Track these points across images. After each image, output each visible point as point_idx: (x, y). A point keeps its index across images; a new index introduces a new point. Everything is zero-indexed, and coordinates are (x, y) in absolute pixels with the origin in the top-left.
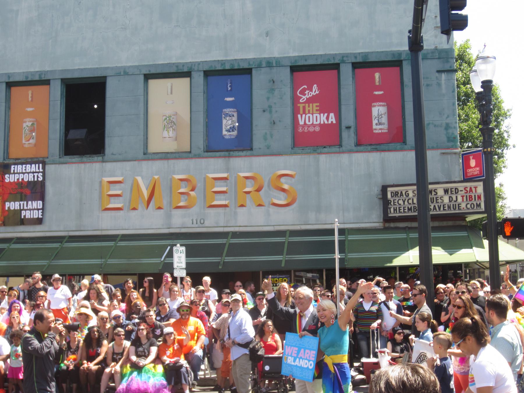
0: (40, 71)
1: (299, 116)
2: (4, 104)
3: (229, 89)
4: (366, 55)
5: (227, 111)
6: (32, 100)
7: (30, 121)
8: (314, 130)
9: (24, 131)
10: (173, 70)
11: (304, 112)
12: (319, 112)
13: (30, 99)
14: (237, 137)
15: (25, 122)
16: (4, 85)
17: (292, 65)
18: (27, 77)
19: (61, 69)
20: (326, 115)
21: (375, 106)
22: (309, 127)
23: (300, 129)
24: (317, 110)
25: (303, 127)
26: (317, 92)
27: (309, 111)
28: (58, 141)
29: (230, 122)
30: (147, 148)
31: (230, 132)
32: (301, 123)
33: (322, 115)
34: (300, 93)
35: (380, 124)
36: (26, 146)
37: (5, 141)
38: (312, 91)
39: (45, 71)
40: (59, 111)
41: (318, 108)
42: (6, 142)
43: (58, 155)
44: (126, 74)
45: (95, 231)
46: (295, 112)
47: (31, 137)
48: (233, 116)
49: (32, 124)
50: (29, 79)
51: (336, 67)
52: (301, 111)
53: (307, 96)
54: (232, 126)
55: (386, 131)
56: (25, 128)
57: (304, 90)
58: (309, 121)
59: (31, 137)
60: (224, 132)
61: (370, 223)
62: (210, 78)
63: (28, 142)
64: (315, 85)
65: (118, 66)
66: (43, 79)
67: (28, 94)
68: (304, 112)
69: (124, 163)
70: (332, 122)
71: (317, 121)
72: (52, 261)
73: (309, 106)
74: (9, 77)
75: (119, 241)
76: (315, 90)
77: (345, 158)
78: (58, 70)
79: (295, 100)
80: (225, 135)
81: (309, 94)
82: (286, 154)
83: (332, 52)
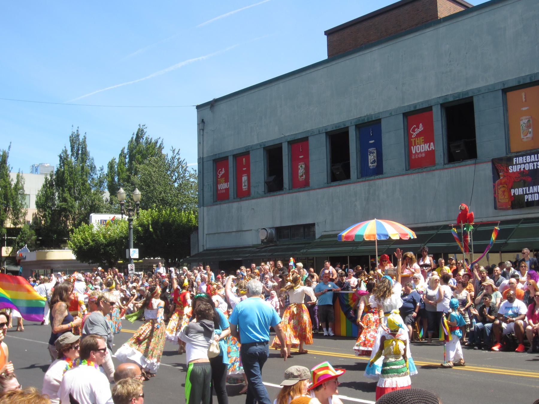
0: (530, 75)
1: (412, 147)
2: (502, 108)
3: (371, 134)
5: (370, 150)
6: (526, 101)
8: (422, 157)
9: (521, 127)
10: (528, 81)
11: (415, 145)
12: (424, 143)
13: (524, 100)
14: (377, 166)
15: (522, 120)
16: (500, 93)
18: (519, 82)
20: (428, 144)
22: (418, 154)
24: (422, 142)
25: (415, 155)
26: (422, 129)
27: (418, 143)
29: (372, 157)
32: (414, 152)
33: (426, 144)
34: (412, 131)
35: (245, 186)
36: (301, 180)
37: (506, 138)
38: (419, 129)
41: (423, 140)
42: (507, 139)
44: (391, 115)
46: (409, 145)
48: (374, 153)
49: (528, 121)
50: (521, 83)
51: (429, 109)
52: (413, 144)
54: (374, 159)
55: (247, 189)
56: (522, 125)
57: (415, 128)
58: (418, 150)
60: (370, 165)
61: (446, 221)
63: (527, 137)
64: (421, 124)
65: (264, 141)
69: (356, 184)
70: (432, 149)
71: (423, 150)
73: (418, 140)
75: (521, 224)
77: (352, 186)
80: (370, 166)
81: (418, 131)
82: (403, 175)
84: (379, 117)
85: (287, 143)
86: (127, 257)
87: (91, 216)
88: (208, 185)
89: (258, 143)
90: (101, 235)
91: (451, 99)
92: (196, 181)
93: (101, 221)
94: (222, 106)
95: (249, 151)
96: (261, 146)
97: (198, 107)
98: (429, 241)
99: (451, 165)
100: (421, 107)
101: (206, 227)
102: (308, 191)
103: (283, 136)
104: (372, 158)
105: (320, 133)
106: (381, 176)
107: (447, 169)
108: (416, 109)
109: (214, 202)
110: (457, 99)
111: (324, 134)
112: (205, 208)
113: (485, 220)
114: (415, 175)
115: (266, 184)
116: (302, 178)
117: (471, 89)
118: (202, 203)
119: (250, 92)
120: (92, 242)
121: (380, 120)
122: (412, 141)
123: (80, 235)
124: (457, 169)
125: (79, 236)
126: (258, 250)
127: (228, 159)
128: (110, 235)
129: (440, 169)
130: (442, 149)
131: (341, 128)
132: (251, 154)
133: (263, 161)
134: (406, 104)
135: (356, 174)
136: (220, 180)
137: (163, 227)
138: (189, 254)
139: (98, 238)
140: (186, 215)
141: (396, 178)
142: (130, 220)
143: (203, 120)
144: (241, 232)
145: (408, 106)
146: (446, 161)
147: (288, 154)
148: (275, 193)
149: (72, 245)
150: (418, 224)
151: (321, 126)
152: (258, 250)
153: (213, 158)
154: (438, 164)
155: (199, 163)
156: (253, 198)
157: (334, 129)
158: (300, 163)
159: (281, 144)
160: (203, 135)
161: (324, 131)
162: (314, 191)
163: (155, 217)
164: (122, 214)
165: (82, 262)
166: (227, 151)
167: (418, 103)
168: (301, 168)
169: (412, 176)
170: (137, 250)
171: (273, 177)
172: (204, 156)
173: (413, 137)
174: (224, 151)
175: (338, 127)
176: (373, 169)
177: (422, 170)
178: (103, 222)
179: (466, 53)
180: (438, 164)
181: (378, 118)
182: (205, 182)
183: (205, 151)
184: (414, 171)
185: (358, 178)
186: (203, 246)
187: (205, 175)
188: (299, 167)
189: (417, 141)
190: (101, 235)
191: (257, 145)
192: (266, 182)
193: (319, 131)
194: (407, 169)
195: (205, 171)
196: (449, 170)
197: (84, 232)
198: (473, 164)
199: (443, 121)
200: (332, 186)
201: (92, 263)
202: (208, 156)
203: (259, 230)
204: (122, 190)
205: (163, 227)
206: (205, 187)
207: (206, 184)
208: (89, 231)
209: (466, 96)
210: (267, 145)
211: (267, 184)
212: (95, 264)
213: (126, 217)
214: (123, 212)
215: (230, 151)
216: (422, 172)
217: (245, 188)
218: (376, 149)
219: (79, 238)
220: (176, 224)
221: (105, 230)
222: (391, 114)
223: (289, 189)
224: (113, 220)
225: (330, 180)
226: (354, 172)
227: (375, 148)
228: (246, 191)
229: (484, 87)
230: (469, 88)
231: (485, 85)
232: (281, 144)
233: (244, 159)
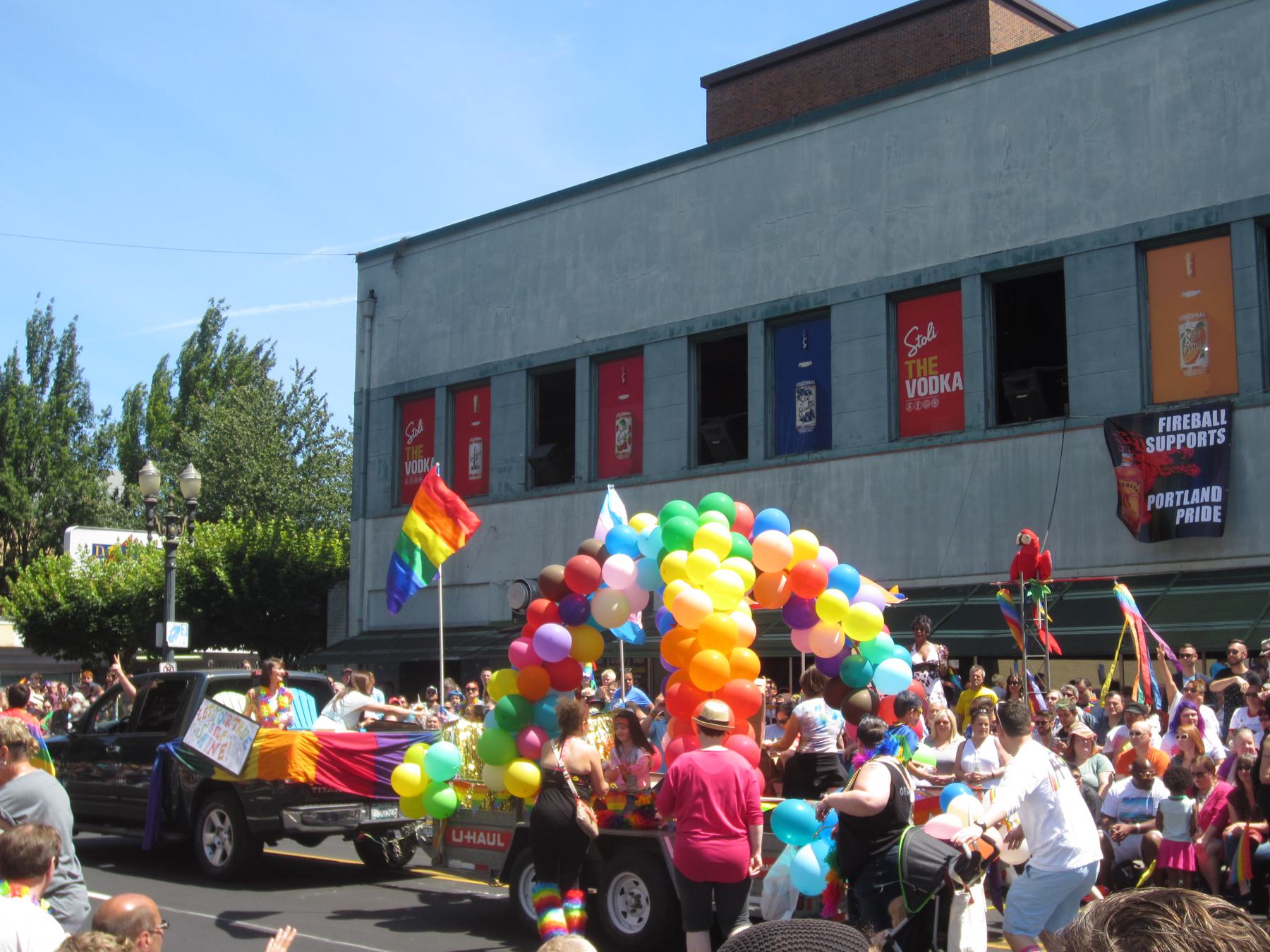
0: (1206, 208)
1: (907, 382)
2: (1134, 290)
3: (805, 346)
4: (918, 275)
5: (801, 385)
6: (1193, 274)
7: (1194, 320)
8: (931, 407)
9: (1181, 341)
10: (1200, 223)
11: (915, 376)
12: (936, 372)
13: (1189, 272)
14: (817, 428)
15: (1183, 322)
16: (1131, 252)
17: (771, 316)
18: (1178, 225)
19: (1252, 196)
20: (948, 375)
21: (471, 443)
22: (922, 401)
23: (910, 407)
24: (934, 369)
25: (914, 402)
26: (934, 336)
27: (922, 371)
28: (1259, 353)
29: (806, 404)
30: (1150, 393)
31: (806, 421)
32: (911, 395)
33: (942, 376)
35: (475, 467)
36: (620, 457)
37: (1141, 367)
38: (926, 336)
39: (1217, 207)
40: (1255, 288)
41: (936, 365)
42: (1145, 369)
43: (1261, 387)
45: (1248, 559)
46: (899, 374)
47: (1197, 354)
48: (810, 393)
49: (1198, 326)
50: (1184, 229)
51: (953, 285)
52: (911, 374)
53: (918, 345)
54: (809, 410)
56: (1183, 335)
57: (915, 334)
58: (923, 391)
59: (1197, 354)
60: (799, 423)
61: (986, 574)
62: (1151, 254)
64: (931, 324)
66: (1214, 224)
67: (1185, 261)
68: (915, 376)
70: (957, 388)
71: (934, 389)
72: (1263, 621)
73: (922, 364)
74: (1141, 231)
75: (1175, 585)
76: (931, 333)
78: (1247, 200)
79: (901, 352)
80: (800, 427)
81: (922, 341)
83: (493, 361)
84: (826, 301)
85: (588, 359)
86: (159, 643)
87: (69, 534)
88: (380, 461)
89: (512, 356)
90: (92, 585)
91: (1008, 263)
92: (349, 452)
93: (94, 546)
94: (424, 258)
95: (489, 378)
96: (520, 364)
97: (362, 258)
98: (941, 624)
99: (1004, 431)
100: (932, 281)
101: (368, 572)
102: (638, 488)
103: (578, 341)
104: (803, 405)
105: (673, 338)
106: (825, 454)
107: (992, 440)
108: (918, 285)
109: (393, 507)
110: (1024, 263)
111: (685, 340)
112: (370, 523)
113: (1084, 574)
114: (912, 453)
115: (529, 466)
116: (622, 454)
117: (1061, 237)
118: (360, 509)
119: (496, 225)
120: (67, 602)
121: (828, 308)
122: (907, 366)
123: (36, 581)
124: (1018, 441)
125: (32, 585)
126: (502, 636)
127: (434, 396)
128: (116, 586)
129: (977, 441)
130: (982, 388)
131: (728, 325)
132: (492, 387)
133: (524, 405)
134: (895, 272)
135: (762, 446)
136: (411, 451)
137: (255, 571)
138: (323, 640)
139: (82, 592)
140: (317, 538)
141: (865, 459)
142: (170, 547)
143: (372, 292)
144: (461, 588)
145: (903, 276)
146: (992, 421)
147: (590, 390)
148: (554, 490)
149: (14, 609)
150: (916, 581)
151: (677, 319)
152: (502, 636)
153: (396, 393)
154: (971, 427)
155: (356, 404)
156: (495, 501)
157: (711, 328)
158: (620, 412)
159: (573, 361)
160: (371, 331)
161: (684, 333)
162: (653, 486)
163: (235, 540)
164: (149, 529)
165: (40, 652)
166: (431, 374)
167: (926, 269)
168: (621, 428)
169: (905, 457)
170: (185, 626)
171: (547, 449)
172: (372, 387)
173: (910, 355)
174: (424, 376)
175: (721, 324)
176: (807, 434)
177: (930, 440)
178: (99, 550)
179: (1050, 148)
180: (971, 427)
181: (823, 305)
182: (371, 454)
183: (375, 372)
184: (910, 444)
185: (766, 457)
186: (361, 621)
187: (372, 435)
188: (618, 423)
189: (919, 367)
190: (92, 585)
191: (510, 362)
192: (529, 460)
193: (672, 332)
194: (894, 438)
195: (373, 427)
196: (998, 444)
197: (47, 576)
198: (1059, 431)
199: (987, 317)
200: (700, 476)
201: (66, 657)
202: (379, 388)
203: (508, 584)
204: (151, 467)
205: (255, 571)
206: (370, 466)
207: (372, 459)
208: (58, 572)
209: (1047, 258)
210: (536, 363)
211: (532, 465)
212: (74, 662)
213: (159, 540)
214: (151, 523)
215: (440, 374)
216: (931, 447)
217: (474, 473)
218: (818, 386)
219: (33, 590)
220: (289, 562)
221: (104, 571)
222: (856, 295)
223: (590, 481)
224: (124, 547)
225: (694, 460)
226: (758, 443)
227: (813, 382)
228: (476, 481)
229: (1092, 234)
230: (1053, 237)
231: (1093, 230)
232: (573, 361)
233: (476, 399)
